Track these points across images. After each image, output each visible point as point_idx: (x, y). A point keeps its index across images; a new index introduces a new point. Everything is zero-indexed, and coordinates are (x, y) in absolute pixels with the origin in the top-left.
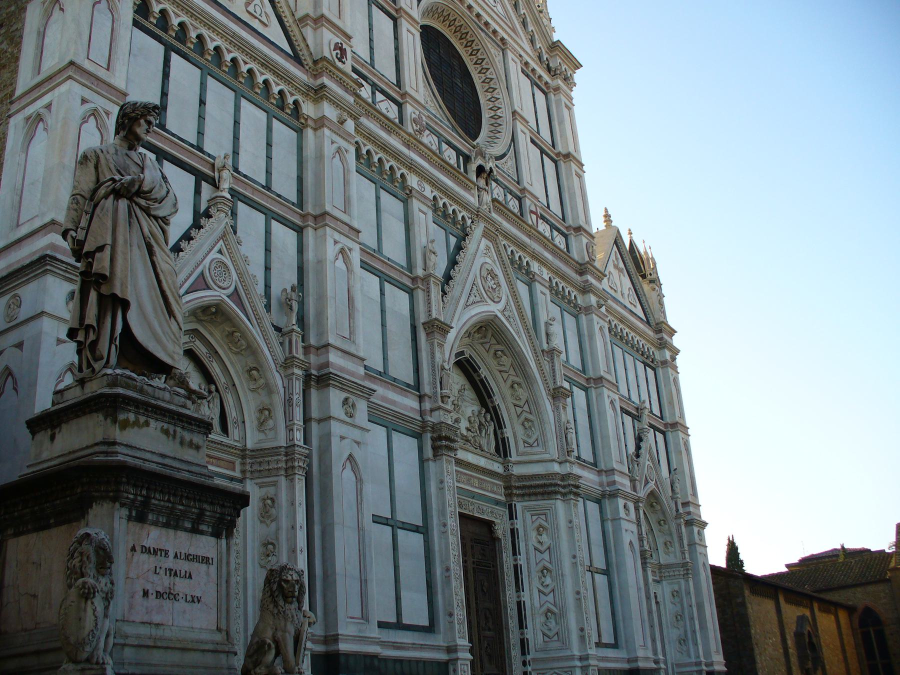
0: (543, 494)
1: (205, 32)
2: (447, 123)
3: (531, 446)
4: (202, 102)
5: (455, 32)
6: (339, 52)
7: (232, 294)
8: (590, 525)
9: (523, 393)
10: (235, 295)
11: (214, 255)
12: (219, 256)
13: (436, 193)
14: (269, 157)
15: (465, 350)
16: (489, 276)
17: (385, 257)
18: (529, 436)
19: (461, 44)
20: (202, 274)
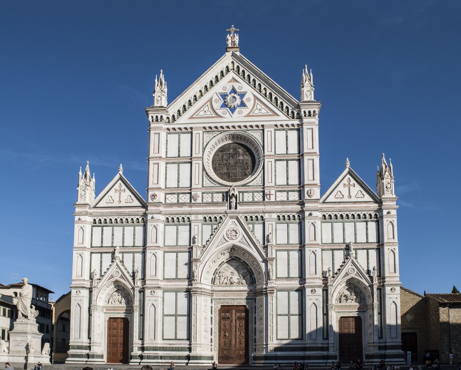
0: (261, 294)
1: (111, 217)
2: (218, 185)
3: (261, 279)
4: (113, 235)
5: (237, 139)
6: (153, 197)
7: (120, 276)
8: (291, 300)
9: (255, 263)
10: (121, 277)
11: (115, 269)
12: (117, 269)
13: (205, 216)
14: (134, 238)
15: (232, 256)
16: (233, 232)
17: (179, 246)
18: (260, 277)
19: (242, 141)
20: (112, 275)
